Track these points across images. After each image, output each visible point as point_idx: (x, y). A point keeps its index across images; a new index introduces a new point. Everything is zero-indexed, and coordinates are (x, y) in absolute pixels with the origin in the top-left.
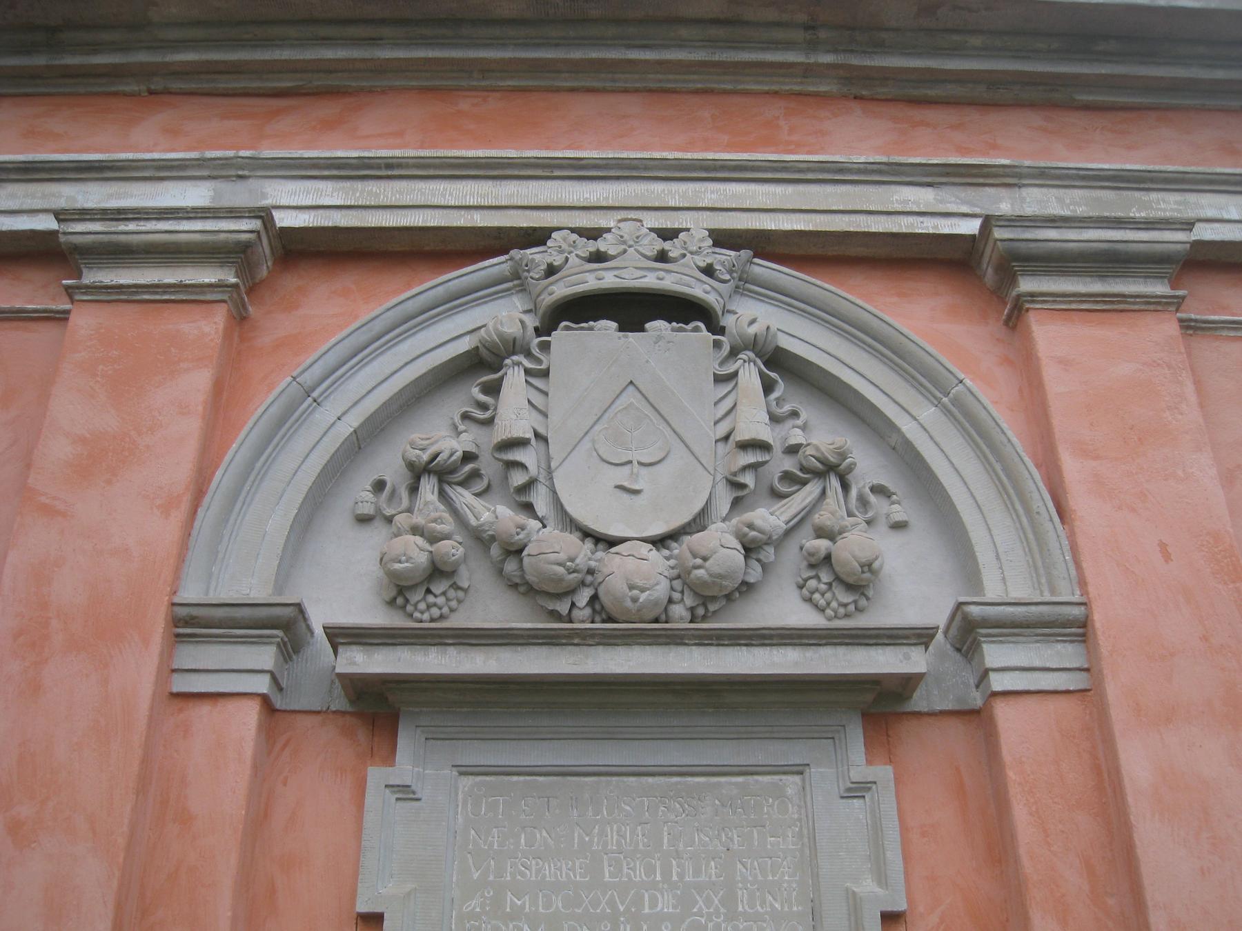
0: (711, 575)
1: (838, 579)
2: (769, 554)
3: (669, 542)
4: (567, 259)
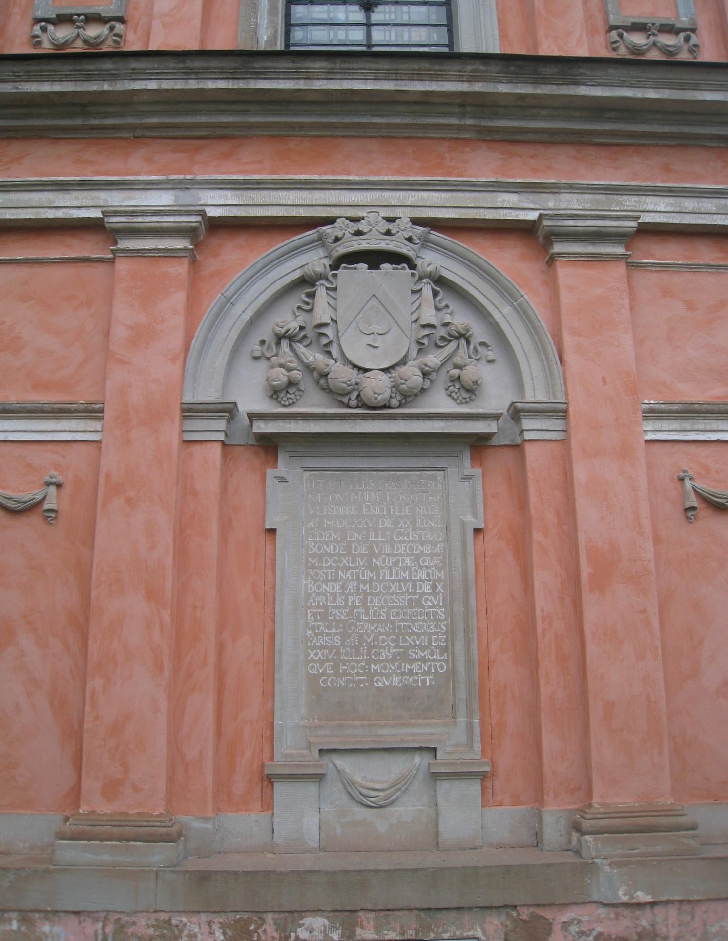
0: (408, 388)
1: (462, 386)
2: (433, 376)
3: (391, 370)
4: (344, 234)
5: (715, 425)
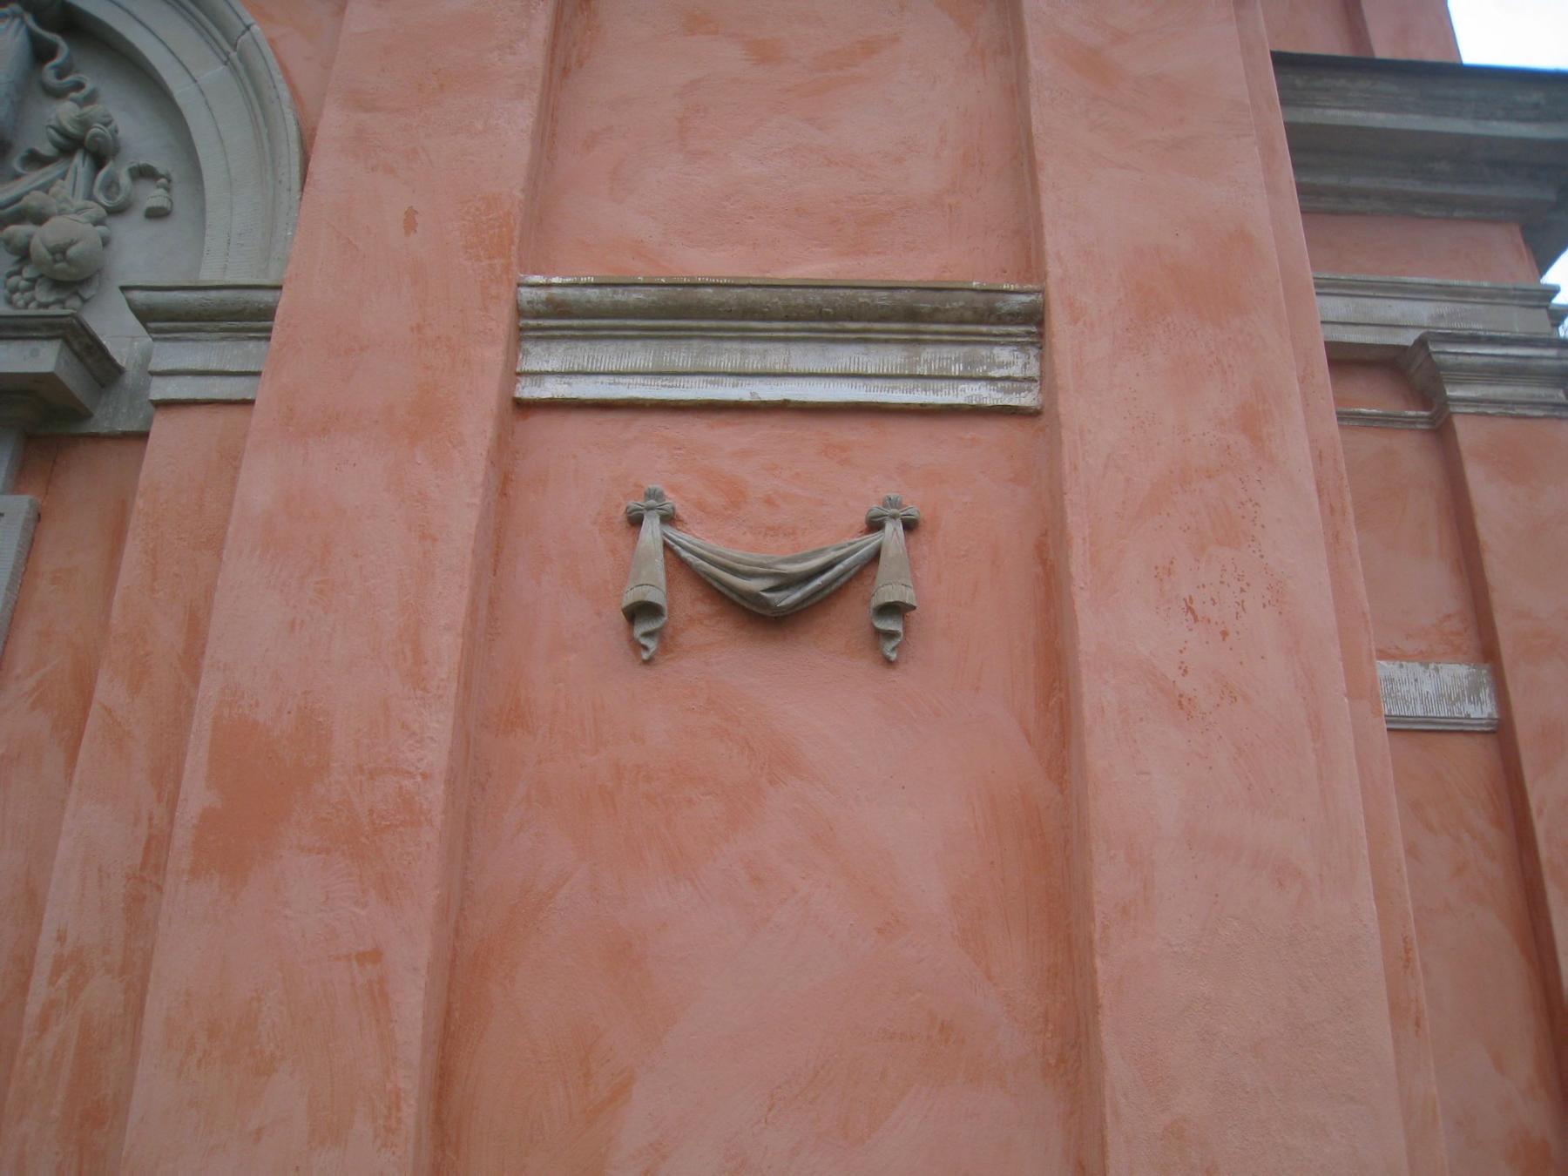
5: (777, 356)
